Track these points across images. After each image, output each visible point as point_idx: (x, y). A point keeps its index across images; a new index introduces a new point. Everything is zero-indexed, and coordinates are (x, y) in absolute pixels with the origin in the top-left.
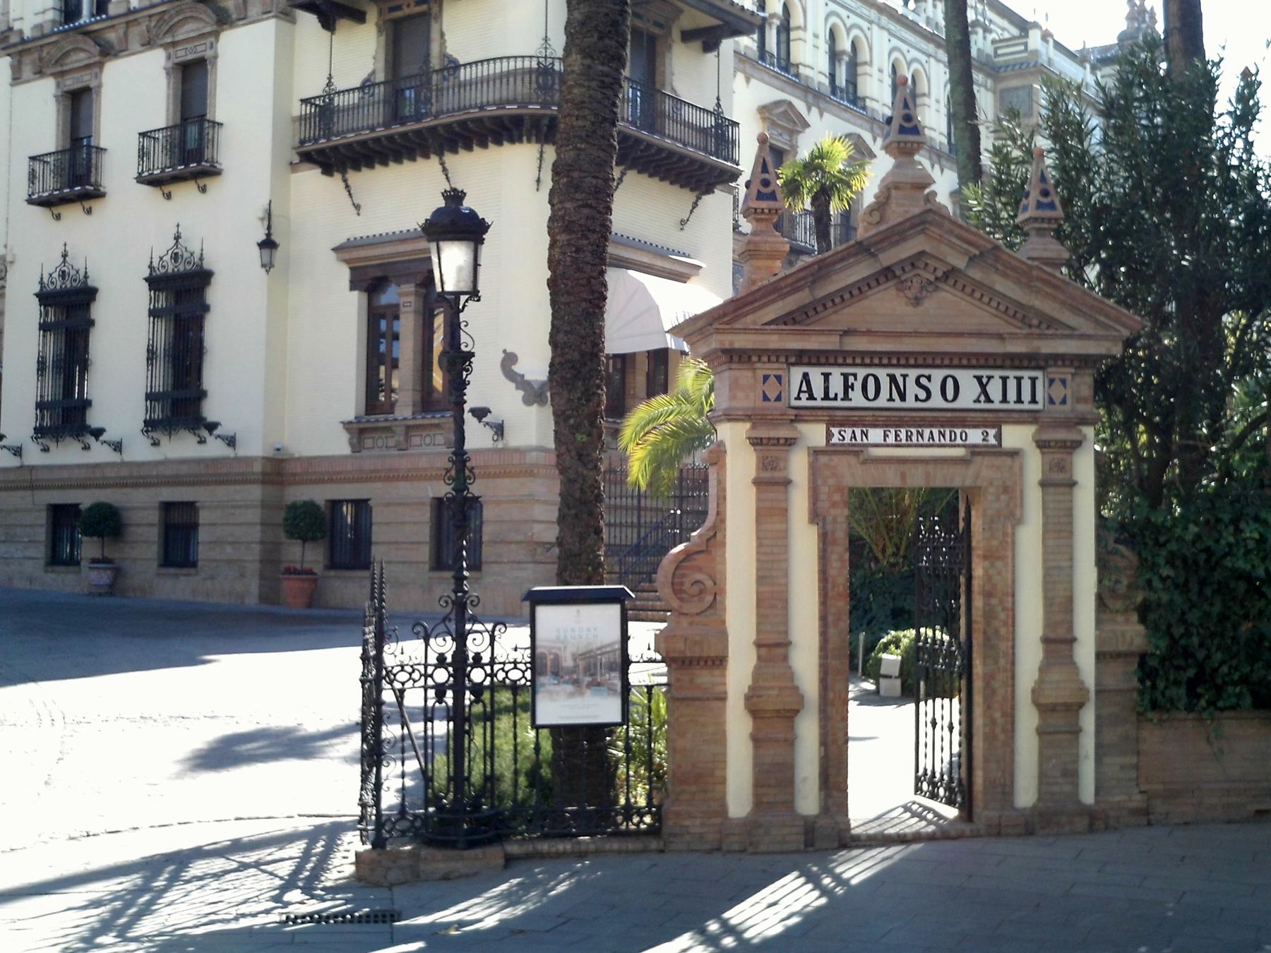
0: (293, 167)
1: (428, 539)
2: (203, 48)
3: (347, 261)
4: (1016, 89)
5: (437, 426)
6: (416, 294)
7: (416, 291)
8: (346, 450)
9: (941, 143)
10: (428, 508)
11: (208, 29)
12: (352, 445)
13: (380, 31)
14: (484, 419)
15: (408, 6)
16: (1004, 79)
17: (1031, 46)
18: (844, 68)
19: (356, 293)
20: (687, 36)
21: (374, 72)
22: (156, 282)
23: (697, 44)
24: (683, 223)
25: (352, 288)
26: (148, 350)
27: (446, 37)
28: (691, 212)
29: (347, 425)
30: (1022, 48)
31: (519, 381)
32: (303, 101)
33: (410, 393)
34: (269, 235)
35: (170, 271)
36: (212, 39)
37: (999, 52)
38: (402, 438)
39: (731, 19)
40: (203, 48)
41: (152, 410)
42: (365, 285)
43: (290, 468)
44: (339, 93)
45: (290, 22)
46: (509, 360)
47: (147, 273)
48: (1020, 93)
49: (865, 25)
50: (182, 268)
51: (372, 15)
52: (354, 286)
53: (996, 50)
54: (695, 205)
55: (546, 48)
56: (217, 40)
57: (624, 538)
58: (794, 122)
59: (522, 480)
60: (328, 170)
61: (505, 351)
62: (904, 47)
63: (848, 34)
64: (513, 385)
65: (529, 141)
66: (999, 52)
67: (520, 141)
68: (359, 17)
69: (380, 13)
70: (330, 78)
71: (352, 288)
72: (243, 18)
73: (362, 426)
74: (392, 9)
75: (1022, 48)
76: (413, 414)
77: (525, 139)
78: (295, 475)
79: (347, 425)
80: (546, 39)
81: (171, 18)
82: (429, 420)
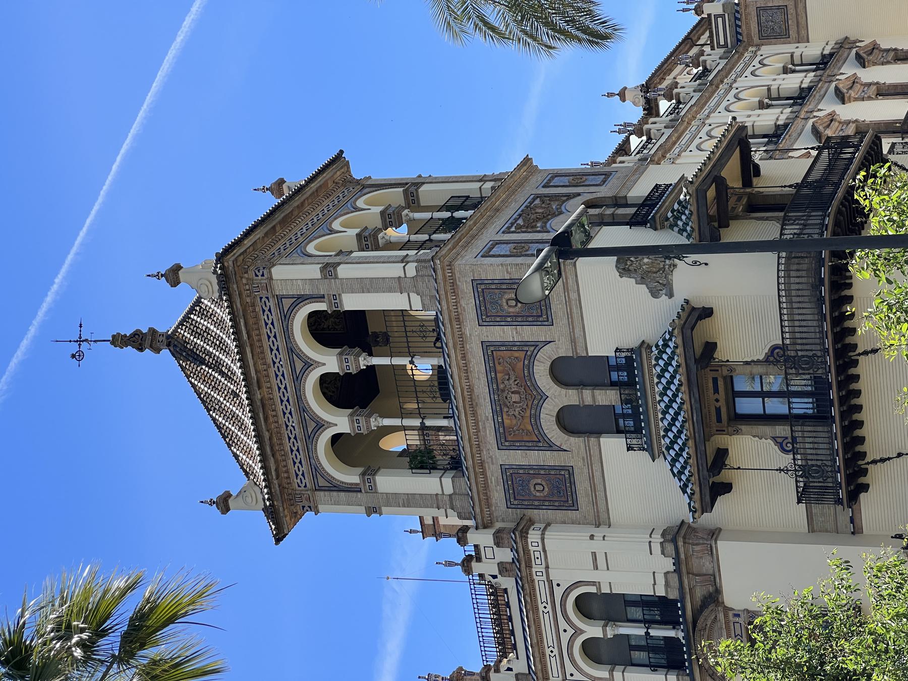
0: (856, 530)
2: (737, 626)
4: (759, 23)
11: (721, 616)
13: (737, 432)
15: (717, 401)
16: (749, 36)
17: (720, 12)
20: (747, 182)
21: (774, 439)
30: (720, 20)
36: (731, 614)
37: (722, 43)
40: (737, 626)
48: (763, 19)
51: (721, 440)
53: (719, 46)
56: (732, 609)
66: (722, 43)
68: (722, 453)
69: (721, 431)
70: (780, 470)
72: (713, 579)
74: (719, 420)
75: (720, 20)
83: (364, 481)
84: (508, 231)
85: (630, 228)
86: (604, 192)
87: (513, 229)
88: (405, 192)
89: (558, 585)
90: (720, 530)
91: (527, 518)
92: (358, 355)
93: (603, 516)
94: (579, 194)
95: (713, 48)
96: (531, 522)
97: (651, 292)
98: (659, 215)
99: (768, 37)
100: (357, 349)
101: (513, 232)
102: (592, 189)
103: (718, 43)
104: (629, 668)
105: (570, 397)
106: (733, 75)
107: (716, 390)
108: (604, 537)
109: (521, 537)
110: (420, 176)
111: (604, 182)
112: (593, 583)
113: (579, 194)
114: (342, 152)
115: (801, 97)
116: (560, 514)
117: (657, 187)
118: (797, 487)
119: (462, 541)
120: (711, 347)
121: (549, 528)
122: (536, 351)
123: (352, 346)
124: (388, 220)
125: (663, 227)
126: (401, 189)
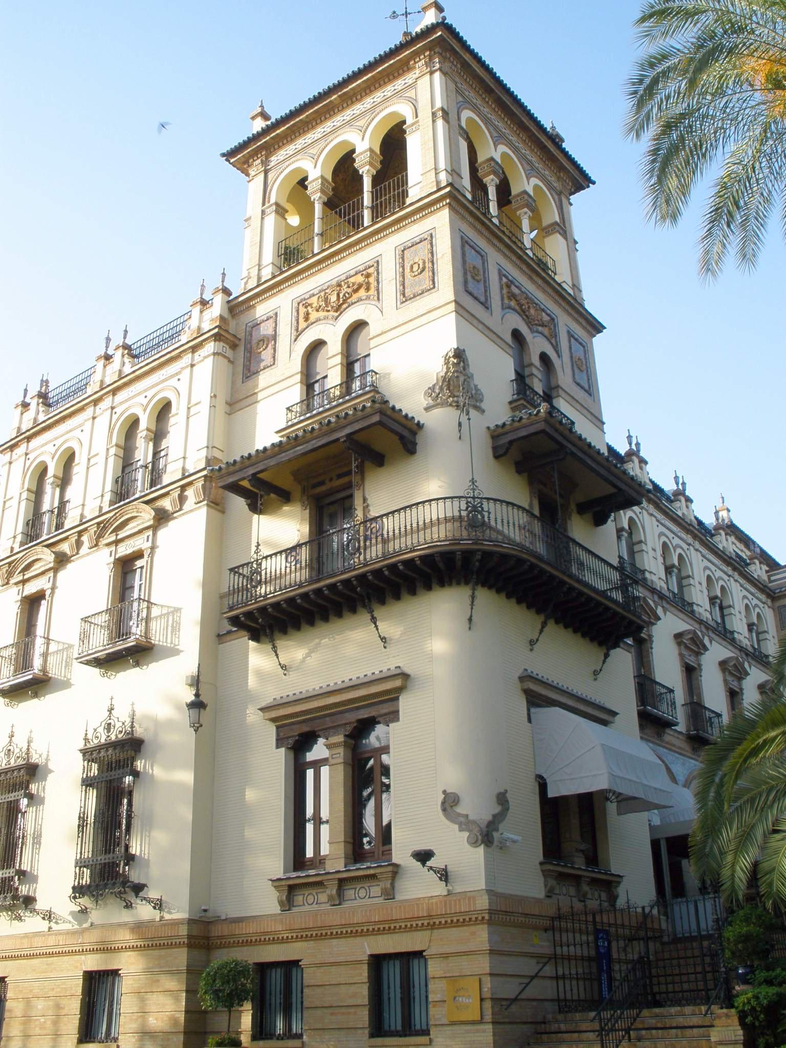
0: (221, 637)
1: (366, 1001)
3: (273, 720)
5: (373, 877)
6: (345, 744)
7: (345, 742)
8: (275, 909)
9: (746, 645)
10: (365, 967)
12: (281, 903)
14: (429, 863)
18: (674, 578)
19: (283, 750)
20: (582, 509)
22: (89, 754)
23: (589, 516)
24: (596, 673)
25: (278, 747)
26: (80, 817)
27: (369, 502)
28: (604, 662)
29: (276, 882)
31: (465, 823)
32: (231, 570)
33: (342, 846)
34: (197, 695)
35: (103, 741)
37: (772, 578)
38: (334, 892)
39: (623, 487)
40: (141, 541)
41: (81, 875)
42: (291, 741)
43: (216, 931)
44: (266, 557)
45: (219, 511)
46: (450, 803)
47: (81, 745)
49: (685, 546)
50: (113, 738)
52: (279, 743)
53: (769, 577)
54: (606, 656)
55: (474, 490)
57: (575, 991)
58: (649, 615)
59: (473, 928)
60: (256, 636)
61: (444, 792)
62: (713, 568)
63: (675, 551)
64: (456, 827)
65: (458, 583)
66: (772, 578)
67: (450, 584)
68: (286, 497)
71: (278, 747)
73: (291, 882)
74: (314, 486)
76: (345, 867)
77: (454, 582)
78: (222, 937)
79: (276, 882)
80: (473, 481)
81: (116, 520)
82: (363, 869)
83: (271, 206)
84: (501, 275)
85: (512, 381)
86: (564, 377)
87: (504, 280)
88: (556, 223)
89: (179, 380)
90: (223, 512)
91: (237, 342)
92: (371, 164)
93: (237, 406)
94: (559, 356)
95: (767, 572)
96: (234, 346)
97: (429, 388)
98: (525, 403)
99: (780, 614)
100: (379, 166)
101: (501, 279)
102: (568, 370)
103: (772, 575)
104: (121, 461)
105: (334, 346)
106: (742, 581)
107: (340, 476)
108: (215, 407)
109: (215, 335)
110: (576, 242)
111: (578, 384)
112: (178, 409)
113: (559, 356)
114: (594, 183)
115: (726, 635)
116: (240, 369)
117: (573, 423)
118: (243, 566)
119: (216, 291)
120: (379, 460)
121: (226, 361)
122: (374, 303)
123: (382, 162)
124: (519, 198)
125: (513, 409)
126: (557, 219)
